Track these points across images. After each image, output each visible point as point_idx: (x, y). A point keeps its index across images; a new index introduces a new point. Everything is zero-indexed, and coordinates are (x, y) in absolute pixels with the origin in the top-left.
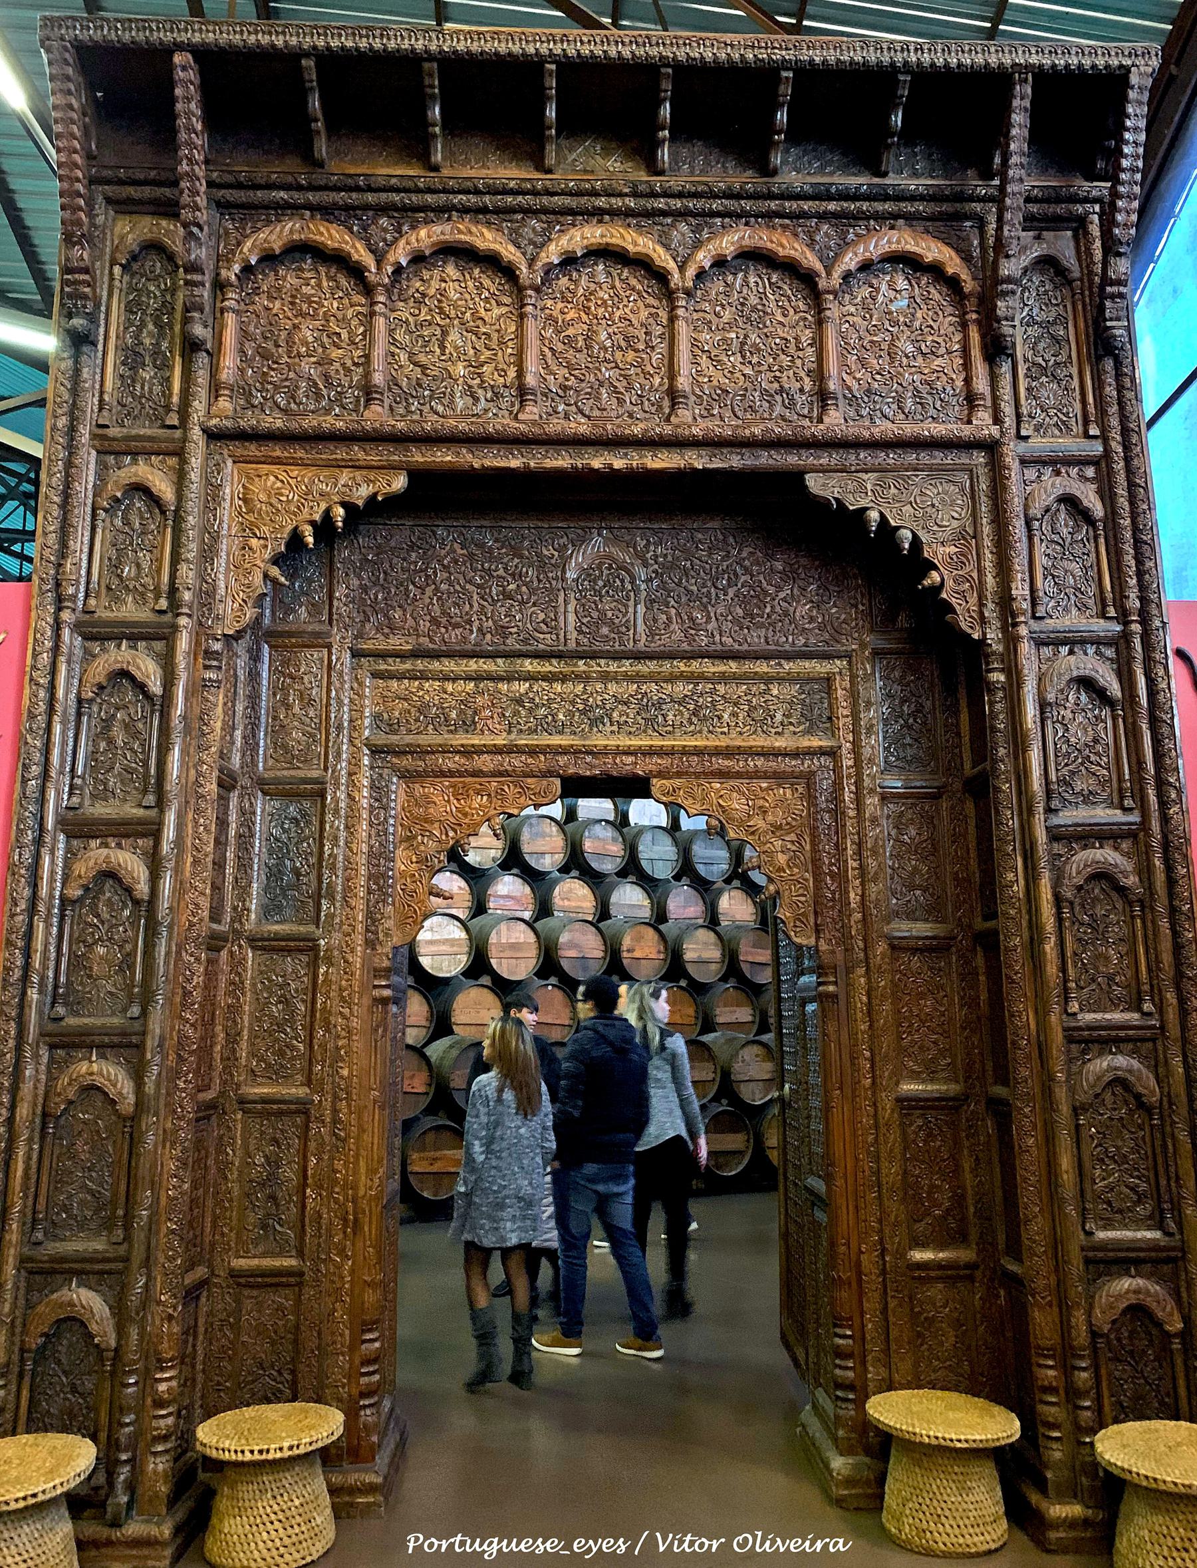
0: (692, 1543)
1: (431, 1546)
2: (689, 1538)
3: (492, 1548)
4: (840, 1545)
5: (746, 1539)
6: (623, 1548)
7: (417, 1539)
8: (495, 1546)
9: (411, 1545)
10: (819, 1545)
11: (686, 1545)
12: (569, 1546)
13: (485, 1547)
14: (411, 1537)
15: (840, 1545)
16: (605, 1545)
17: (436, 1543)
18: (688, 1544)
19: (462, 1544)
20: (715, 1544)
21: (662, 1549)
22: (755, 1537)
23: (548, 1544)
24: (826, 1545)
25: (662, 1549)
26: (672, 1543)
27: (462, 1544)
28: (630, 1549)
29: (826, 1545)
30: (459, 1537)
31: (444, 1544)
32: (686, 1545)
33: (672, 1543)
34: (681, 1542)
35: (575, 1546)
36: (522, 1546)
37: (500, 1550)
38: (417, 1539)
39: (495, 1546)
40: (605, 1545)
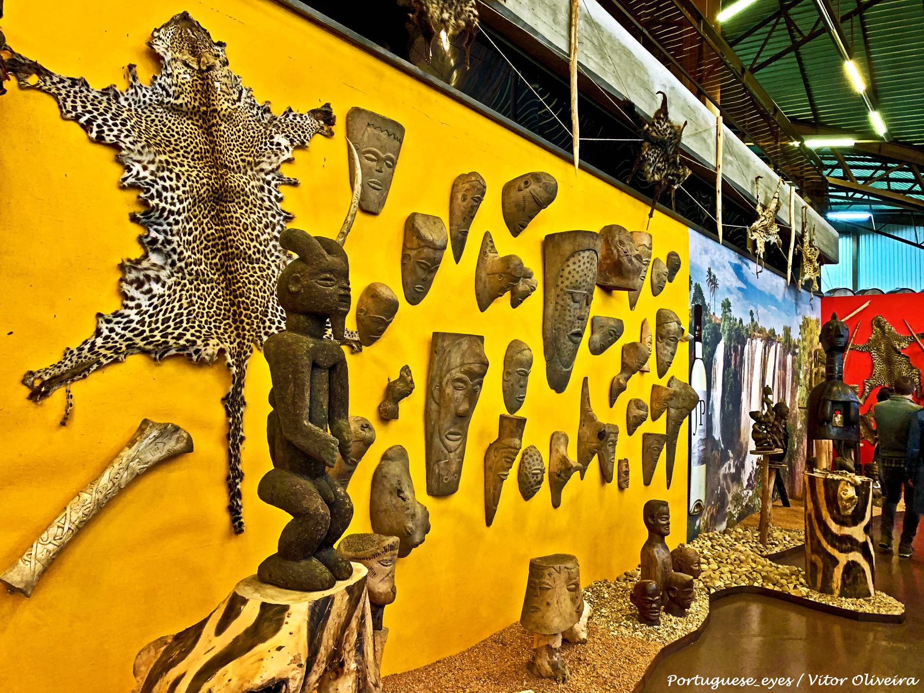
0: (829, 680)
1: (681, 681)
2: (827, 677)
3: (716, 683)
4: (913, 681)
5: (859, 678)
7: (673, 678)
8: (718, 682)
9: (670, 681)
10: (901, 681)
11: (825, 681)
13: (712, 682)
14: (670, 677)
15: (913, 681)
18: (827, 681)
19: (699, 680)
20: (842, 681)
21: (812, 684)
22: (864, 677)
25: (812, 684)
27: (699, 680)
28: (794, 684)
29: (904, 683)
30: (697, 677)
31: (689, 681)
32: (825, 681)
34: (823, 680)
35: (763, 682)
36: (733, 682)
37: (720, 684)
38: (673, 678)
39: (718, 682)
40: (780, 681)
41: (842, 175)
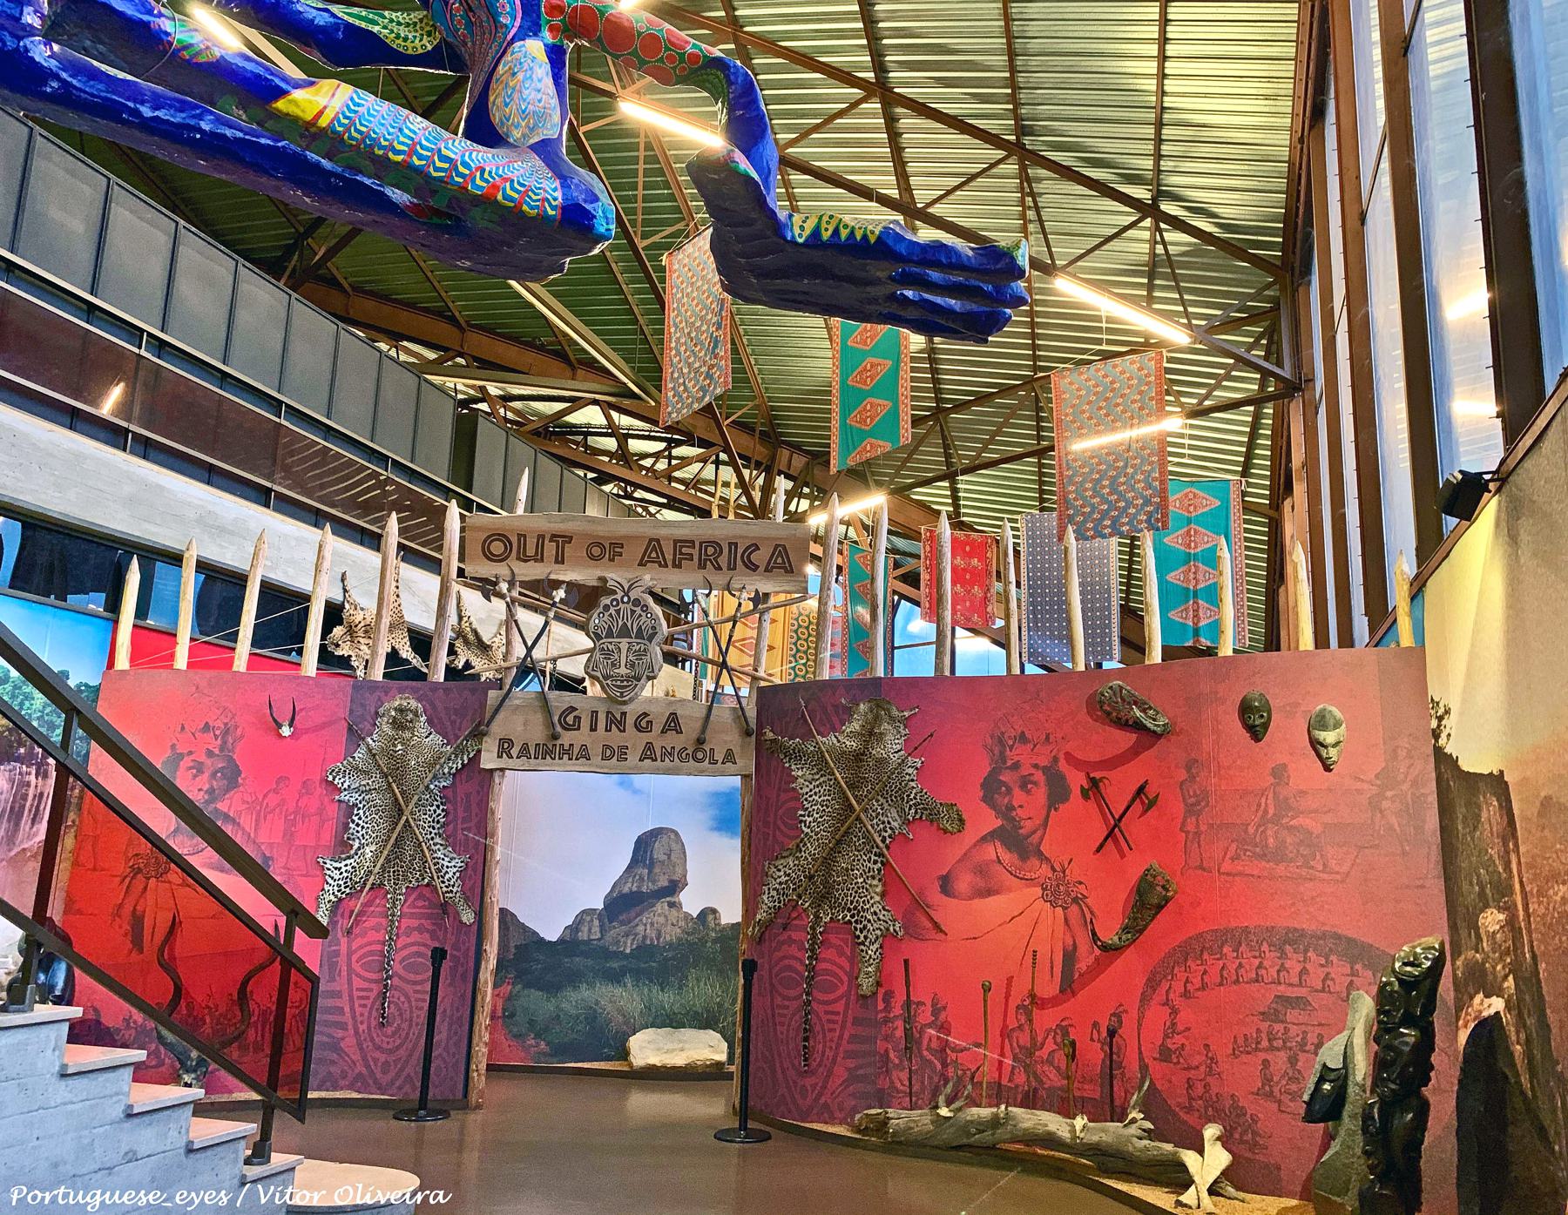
3: (95, 1199)
4: (440, 1197)
6: (225, 1200)
8: (98, 1198)
9: (15, 1197)
11: (287, 1197)
12: (170, 1199)
13: (88, 1199)
15: (440, 1197)
16: (208, 1197)
17: (40, 1195)
19: (66, 1196)
23: (151, 1197)
24: (427, 1197)
26: (274, 1195)
27: (66, 1196)
28: (232, 1201)
30: (62, 1190)
32: (287, 1197)
33: (274, 1195)
34: (283, 1194)
36: (125, 1198)
37: (103, 1202)
39: (98, 1198)
40: (208, 1197)
41: (630, 441)
